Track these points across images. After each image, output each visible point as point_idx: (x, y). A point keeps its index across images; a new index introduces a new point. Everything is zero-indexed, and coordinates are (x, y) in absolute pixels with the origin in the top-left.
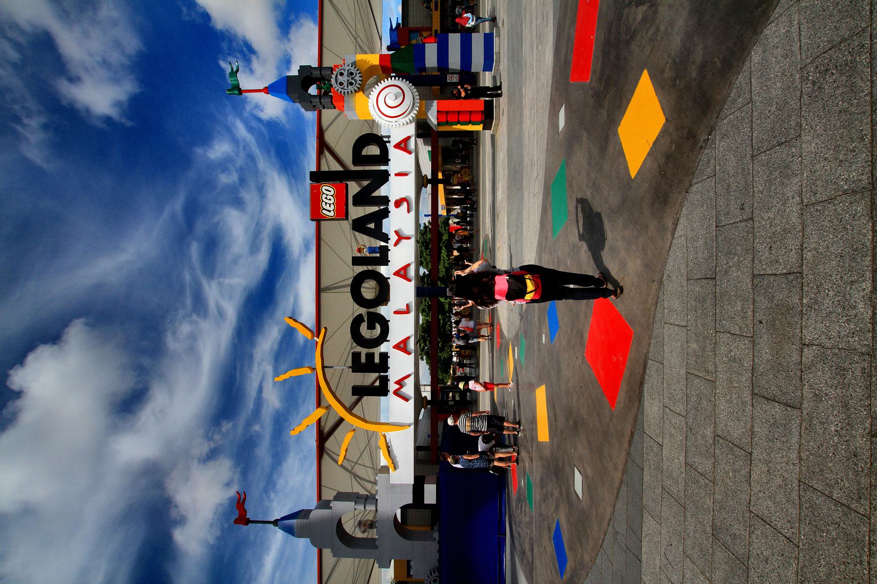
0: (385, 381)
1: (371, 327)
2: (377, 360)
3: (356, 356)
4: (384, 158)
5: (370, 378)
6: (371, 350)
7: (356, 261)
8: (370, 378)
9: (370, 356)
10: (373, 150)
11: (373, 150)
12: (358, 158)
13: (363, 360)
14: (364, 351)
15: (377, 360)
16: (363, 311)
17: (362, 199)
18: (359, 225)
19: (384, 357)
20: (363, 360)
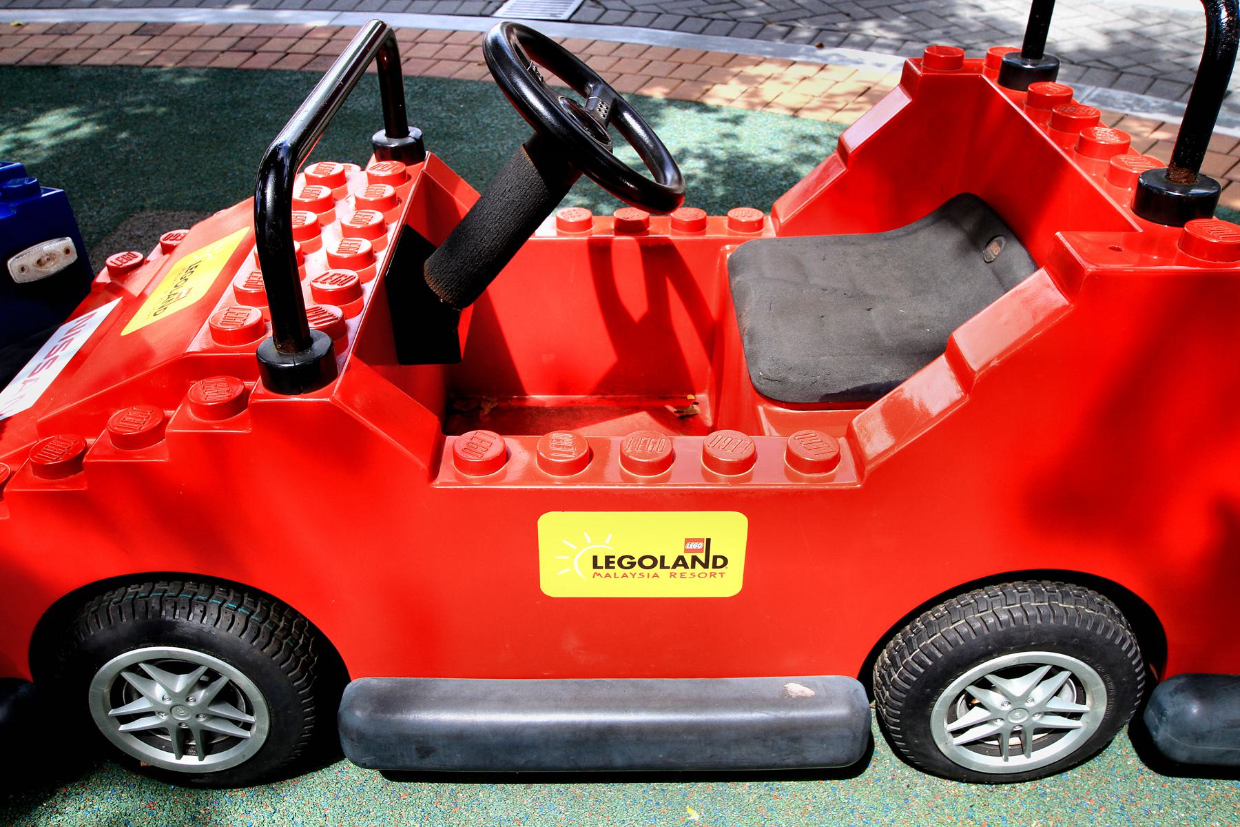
0: (601, 568)
1: (628, 563)
2: (611, 565)
3: (614, 557)
4: (715, 566)
5: (601, 562)
6: (616, 562)
7: (662, 558)
8: (601, 562)
9: (613, 562)
10: (720, 562)
11: (720, 562)
12: (715, 558)
13: (611, 560)
14: (616, 560)
15: (611, 565)
16: (636, 560)
17: (695, 559)
18: (681, 558)
19: (613, 568)
20: (611, 560)
